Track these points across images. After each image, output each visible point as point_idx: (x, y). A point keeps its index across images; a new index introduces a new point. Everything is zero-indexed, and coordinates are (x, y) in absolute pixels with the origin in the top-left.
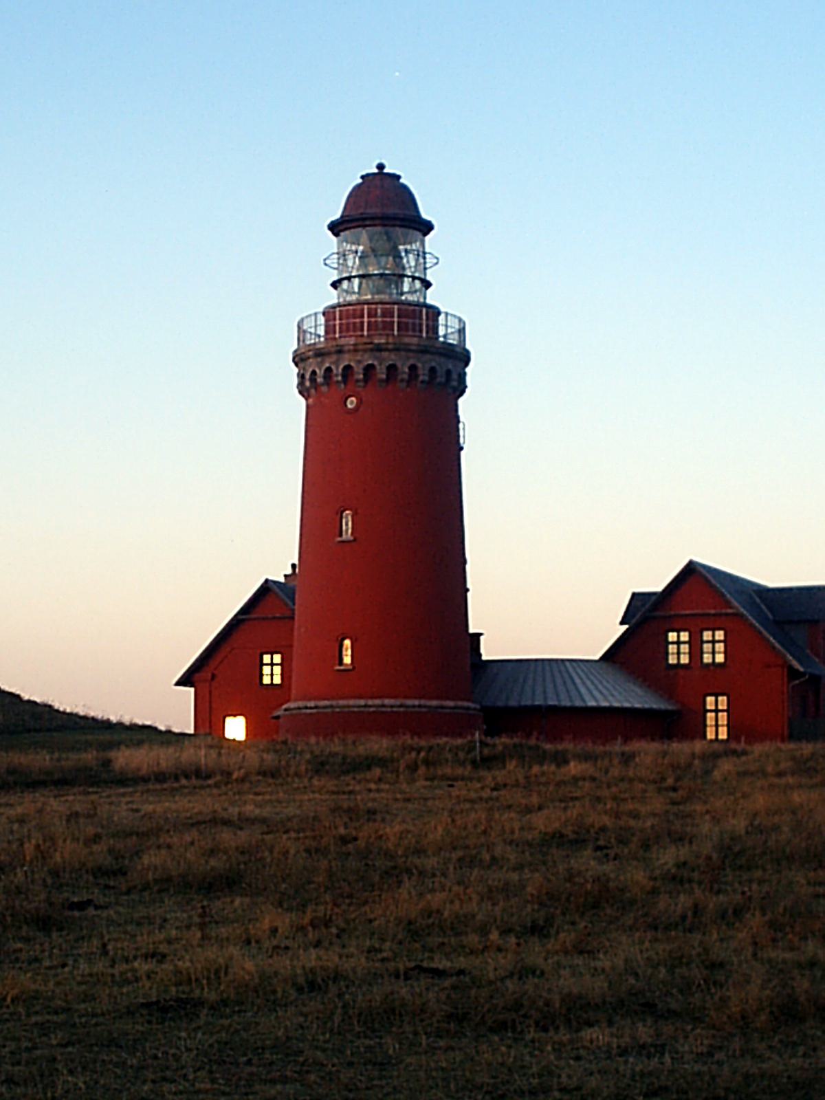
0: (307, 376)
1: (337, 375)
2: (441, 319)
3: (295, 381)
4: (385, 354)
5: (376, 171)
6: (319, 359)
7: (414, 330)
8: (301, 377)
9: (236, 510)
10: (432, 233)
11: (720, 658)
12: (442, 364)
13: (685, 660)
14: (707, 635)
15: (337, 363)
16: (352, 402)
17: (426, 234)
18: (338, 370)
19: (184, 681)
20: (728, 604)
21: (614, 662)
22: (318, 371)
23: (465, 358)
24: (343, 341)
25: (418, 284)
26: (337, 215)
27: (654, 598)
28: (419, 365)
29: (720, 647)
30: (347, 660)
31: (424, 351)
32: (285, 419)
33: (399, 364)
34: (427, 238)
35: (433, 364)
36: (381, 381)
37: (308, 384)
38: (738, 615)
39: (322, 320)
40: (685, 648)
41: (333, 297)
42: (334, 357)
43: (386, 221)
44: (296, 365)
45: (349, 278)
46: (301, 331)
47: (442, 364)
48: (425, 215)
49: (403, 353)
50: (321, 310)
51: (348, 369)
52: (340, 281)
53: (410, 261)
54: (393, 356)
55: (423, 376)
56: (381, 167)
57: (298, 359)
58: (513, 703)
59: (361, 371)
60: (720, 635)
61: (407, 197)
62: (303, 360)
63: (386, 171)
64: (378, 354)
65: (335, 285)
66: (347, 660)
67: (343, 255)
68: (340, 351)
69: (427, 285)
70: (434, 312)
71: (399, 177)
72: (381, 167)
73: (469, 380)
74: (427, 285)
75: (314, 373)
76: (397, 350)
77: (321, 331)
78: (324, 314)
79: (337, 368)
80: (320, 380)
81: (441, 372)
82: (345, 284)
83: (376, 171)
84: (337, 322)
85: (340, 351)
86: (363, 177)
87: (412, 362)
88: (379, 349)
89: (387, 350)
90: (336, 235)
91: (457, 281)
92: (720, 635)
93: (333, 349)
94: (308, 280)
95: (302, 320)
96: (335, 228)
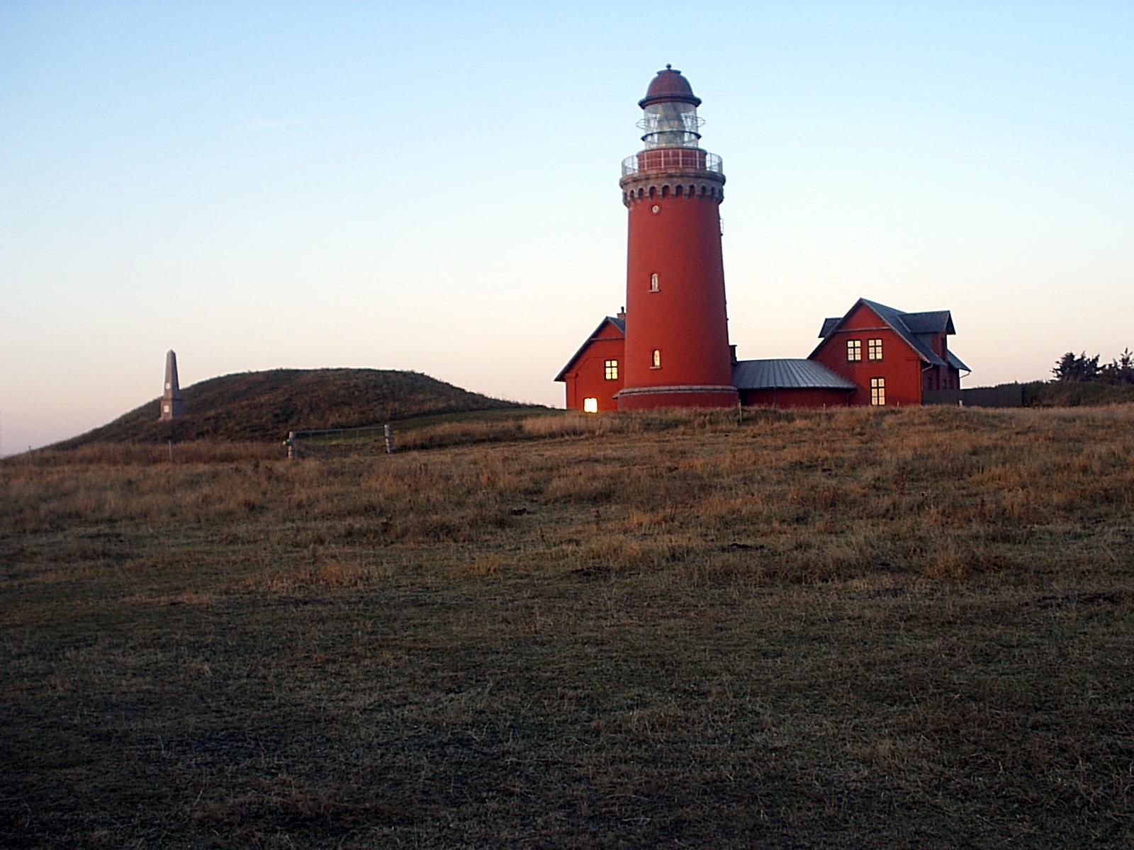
0: (629, 194)
2: (708, 157)
3: (621, 197)
4: (675, 179)
5: (666, 69)
7: (692, 164)
8: (625, 194)
9: (588, 277)
10: (701, 105)
11: (879, 356)
12: (710, 185)
13: (858, 358)
14: (871, 343)
15: (645, 185)
17: (697, 106)
18: (647, 190)
19: (560, 378)
20: (884, 324)
21: (816, 360)
23: (723, 181)
24: (649, 172)
25: (693, 137)
26: (643, 96)
27: (839, 322)
28: (695, 185)
29: (879, 349)
30: (657, 363)
31: (697, 177)
32: (617, 219)
33: (683, 185)
34: (698, 108)
35: (703, 184)
36: (672, 195)
37: (629, 198)
38: (890, 330)
39: (636, 160)
40: (858, 351)
41: (642, 146)
42: (644, 182)
43: (673, 99)
44: (622, 187)
45: (652, 134)
46: (624, 168)
47: (710, 185)
48: (696, 94)
50: (635, 154)
52: (646, 136)
53: (688, 124)
55: (698, 191)
56: (669, 66)
57: (623, 184)
58: (756, 386)
60: (879, 342)
61: (685, 84)
62: (625, 184)
63: (672, 68)
65: (643, 139)
66: (657, 363)
67: (648, 121)
69: (699, 137)
70: (703, 154)
71: (679, 72)
72: (669, 66)
73: (725, 194)
74: (699, 137)
75: (632, 192)
76: (682, 176)
77: (636, 167)
78: (637, 156)
80: (636, 196)
81: (709, 188)
82: (649, 138)
83: (666, 69)
85: (648, 179)
86: (658, 73)
87: (691, 183)
88: (671, 176)
89: (677, 177)
90: (643, 108)
91: (717, 134)
92: (879, 342)
94: (627, 136)
95: (624, 161)
96: (643, 104)
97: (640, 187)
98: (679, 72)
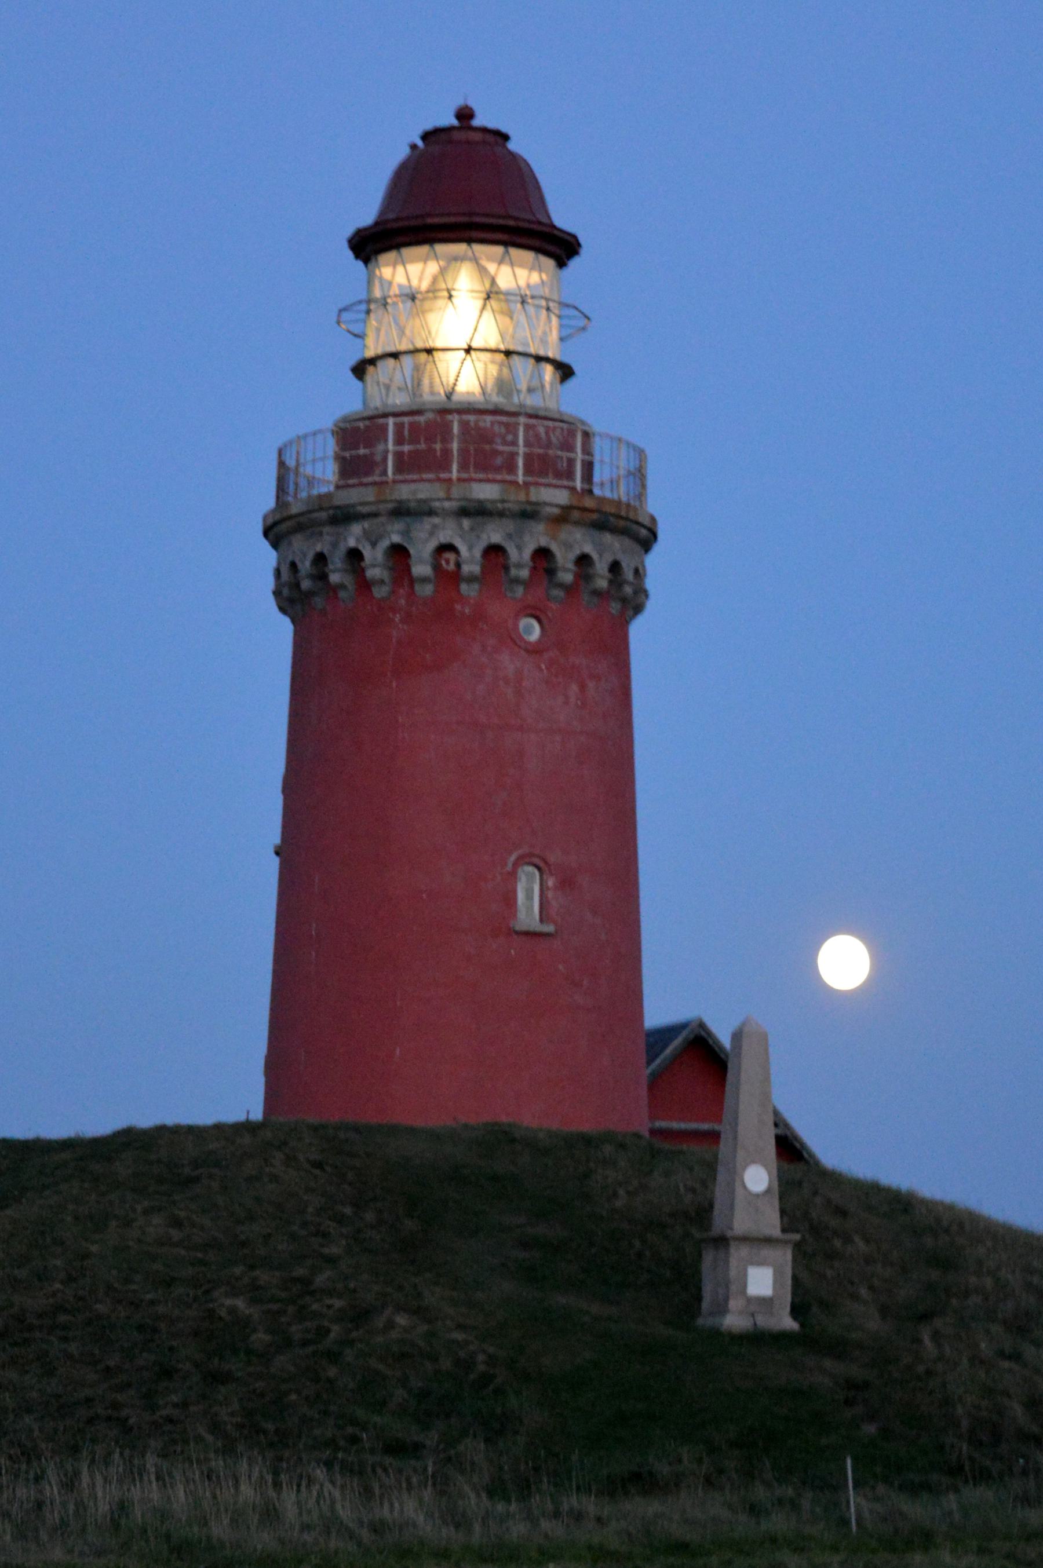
1: (519, 566)
4: (608, 538)
5: (455, 122)
6: (466, 523)
16: (529, 630)
18: (520, 556)
22: (463, 549)
42: (510, 525)
49: (627, 542)
51: (543, 554)
54: (617, 545)
56: (465, 115)
59: (571, 566)
63: (476, 122)
64: (596, 533)
68: (529, 514)
72: (465, 115)
83: (455, 122)
85: (529, 514)
93: (515, 508)
97: (496, 538)
98: (505, 137)
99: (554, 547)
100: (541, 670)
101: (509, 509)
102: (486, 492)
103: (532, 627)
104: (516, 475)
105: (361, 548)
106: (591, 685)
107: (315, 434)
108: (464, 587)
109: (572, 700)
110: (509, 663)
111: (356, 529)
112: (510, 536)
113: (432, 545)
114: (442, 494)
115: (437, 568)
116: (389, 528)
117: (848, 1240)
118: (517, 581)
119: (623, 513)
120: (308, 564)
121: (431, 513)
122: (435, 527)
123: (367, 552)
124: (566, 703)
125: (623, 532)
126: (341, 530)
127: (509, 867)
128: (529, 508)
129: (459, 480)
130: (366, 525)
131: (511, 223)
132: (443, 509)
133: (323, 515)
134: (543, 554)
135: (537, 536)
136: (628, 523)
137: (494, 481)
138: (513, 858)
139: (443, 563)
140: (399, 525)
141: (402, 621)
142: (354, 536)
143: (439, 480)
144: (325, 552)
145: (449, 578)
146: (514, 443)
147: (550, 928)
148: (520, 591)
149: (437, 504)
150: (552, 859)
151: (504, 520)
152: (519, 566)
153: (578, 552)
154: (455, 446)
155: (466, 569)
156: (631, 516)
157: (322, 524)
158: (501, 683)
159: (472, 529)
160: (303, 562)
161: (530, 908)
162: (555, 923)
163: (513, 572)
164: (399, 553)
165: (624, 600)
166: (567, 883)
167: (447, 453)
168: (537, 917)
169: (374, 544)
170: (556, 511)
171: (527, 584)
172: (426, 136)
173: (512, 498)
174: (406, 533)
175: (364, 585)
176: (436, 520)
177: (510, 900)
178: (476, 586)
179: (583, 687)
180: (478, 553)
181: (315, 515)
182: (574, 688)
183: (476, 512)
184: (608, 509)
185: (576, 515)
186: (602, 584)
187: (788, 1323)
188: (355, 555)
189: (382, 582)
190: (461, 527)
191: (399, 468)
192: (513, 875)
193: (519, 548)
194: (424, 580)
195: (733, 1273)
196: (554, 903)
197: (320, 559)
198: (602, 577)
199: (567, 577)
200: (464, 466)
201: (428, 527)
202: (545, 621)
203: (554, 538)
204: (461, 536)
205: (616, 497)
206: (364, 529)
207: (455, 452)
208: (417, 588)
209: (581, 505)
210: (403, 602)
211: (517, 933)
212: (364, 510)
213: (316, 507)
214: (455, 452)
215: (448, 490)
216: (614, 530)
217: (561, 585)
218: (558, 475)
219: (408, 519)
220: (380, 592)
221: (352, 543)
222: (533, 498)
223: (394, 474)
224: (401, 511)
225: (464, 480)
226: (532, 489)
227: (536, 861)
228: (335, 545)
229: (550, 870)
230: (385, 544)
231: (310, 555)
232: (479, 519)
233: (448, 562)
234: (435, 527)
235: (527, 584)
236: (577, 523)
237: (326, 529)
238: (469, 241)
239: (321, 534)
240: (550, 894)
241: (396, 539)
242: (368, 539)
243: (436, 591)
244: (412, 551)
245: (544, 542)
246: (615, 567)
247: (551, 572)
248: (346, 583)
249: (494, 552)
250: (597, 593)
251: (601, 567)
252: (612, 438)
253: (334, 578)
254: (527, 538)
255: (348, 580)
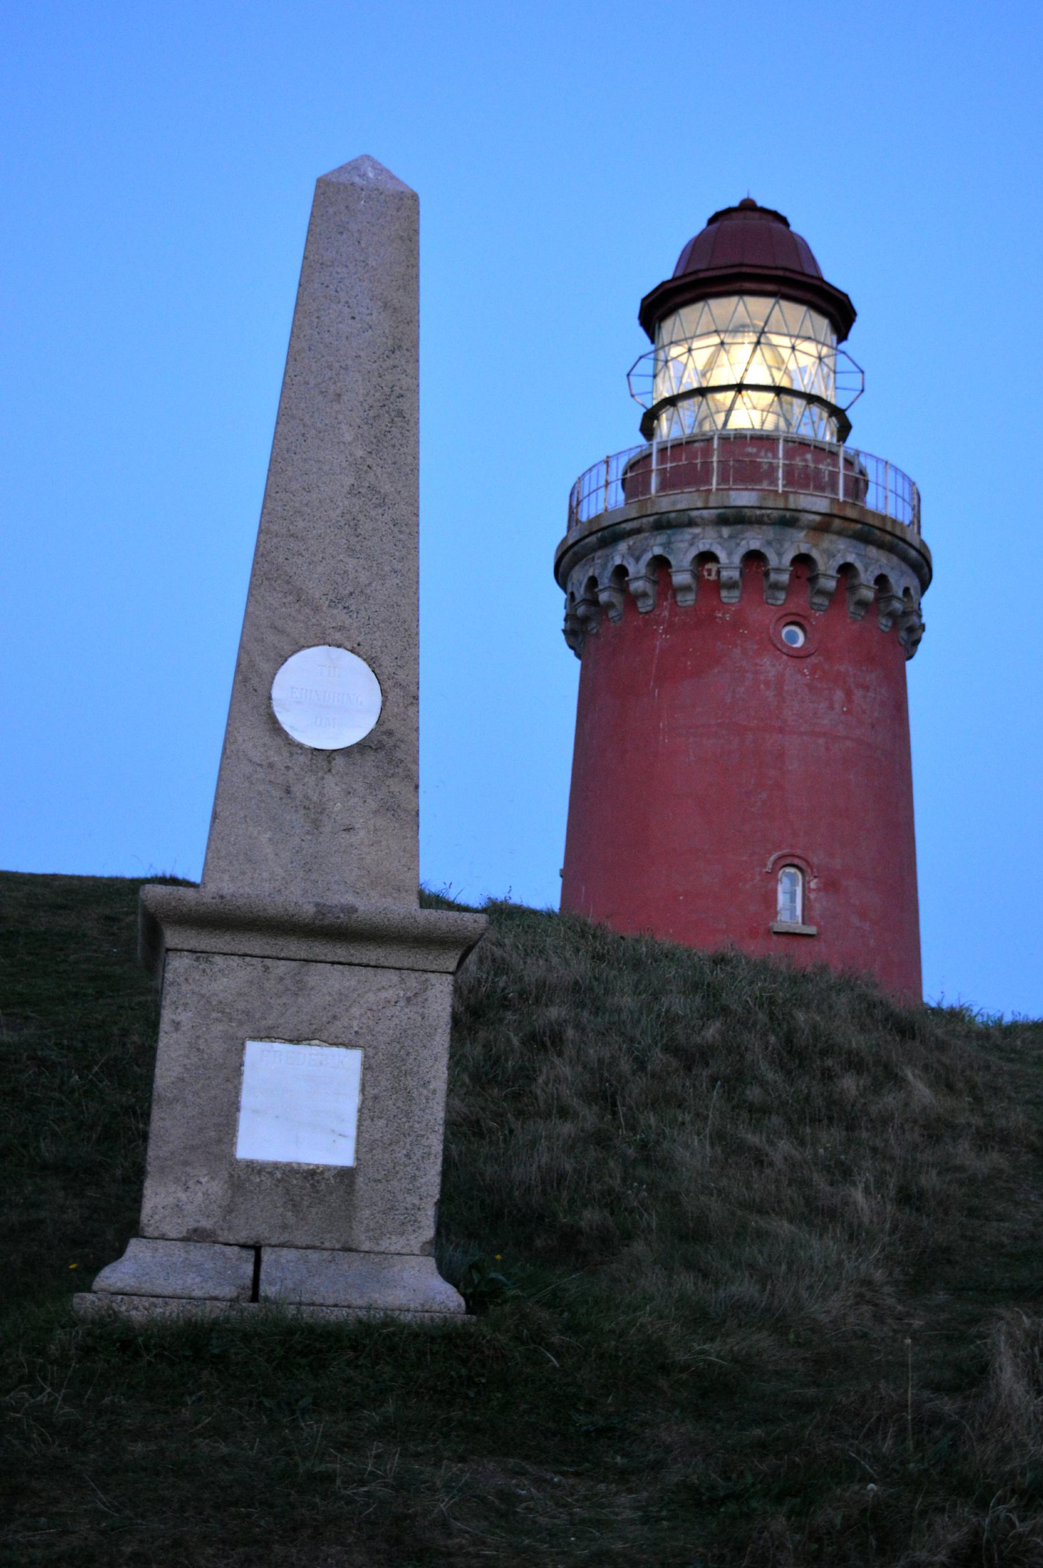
1: (778, 570)
4: (873, 551)
6: (726, 531)
16: (793, 637)
26: (663, 268)
33: (893, 578)
42: (770, 532)
49: (895, 560)
51: (803, 561)
64: (862, 546)
68: (788, 521)
79: (780, 555)
84: (781, 462)
85: (788, 521)
93: (775, 514)
97: (755, 545)
99: (815, 554)
100: (806, 676)
101: (768, 516)
102: (744, 498)
103: (795, 633)
104: (777, 485)
105: (625, 564)
106: (858, 694)
107: (590, 470)
108: (724, 593)
109: (837, 706)
110: (770, 666)
111: (623, 547)
112: (769, 543)
113: (693, 553)
114: (700, 505)
115: (697, 576)
116: (652, 542)
117: (889, 1077)
118: (776, 586)
119: (889, 528)
120: (582, 590)
121: (691, 523)
122: (695, 536)
123: (632, 569)
124: (831, 707)
125: (891, 549)
126: (607, 551)
127: (769, 867)
128: (788, 514)
129: (717, 490)
130: (631, 541)
131: (780, 273)
132: (703, 519)
133: (593, 539)
134: (803, 561)
135: (798, 543)
136: (896, 541)
137: (753, 489)
138: (772, 858)
139: (705, 573)
140: (661, 538)
141: (666, 632)
142: (619, 555)
143: (698, 491)
144: (596, 575)
145: (709, 588)
146: (775, 456)
147: (812, 930)
148: (782, 596)
149: (695, 513)
150: (815, 860)
151: (764, 527)
152: (778, 570)
153: (842, 562)
154: (715, 459)
155: (725, 574)
156: (898, 533)
157: (594, 549)
158: (762, 686)
159: (731, 537)
160: (578, 590)
161: (793, 910)
162: (818, 925)
163: (773, 577)
164: (661, 564)
165: (891, 615)
166: (831, 885)
167: (707, 465)
168: (800, 920)
169: (637, 559)
170: (818, 518)
171: (788, 589)
172: (712, 221)
173: (770, 504)
174: (667, 545)
175: (631, 600)
176: (697, 530)
177: (769, 900)
178: (736, 593)
179: (849, 694)
180: (737, 560)
181: (587, 540)
182: (839, 695)
183: (734, 519)
184: (870, 520)
185: (837, 523)
186: (869, 595)
187: (418, 1287)
188: (621, 571)
189: (645, 595)
190: (721, 536)
191: (663, 486)
192: (772, 876)
193: (780, 555)
194: (686, 589)
195: (171, 1060)
196: (817, 906)
197: (593, 582)
198: (868, 587)
199: (831, 584)
200: (723, 479)
201: (688, 537)
202: (808, 628)
203: (816, 546)
204: (720, 544)
205: (883, 512)
206: (630, 548)
207: (715, 465)
208: (679, 598)
209: (841, 514)
210: (666, 613)
211: (776, 933)
212: (628, 526)
213: (586, 533)
214: (715, 465)
215: (707, 501)
216: (880, 545)
217: (821, 592)
218: (820, 487)
219: (669, 532)
220: (644, 606)
221: (618, 561)
222: (792, 506)
223: (657, 491)
224: (663, 524)
225: (723, 490)
226: (791, 497)
227: (796, 861)
228: (604, 566)
229: (812, 872)
230: (647, 557)
231: (585, 581)
232: (739, 527)
233: (709, 571)
234: (695, 536)
235: (788, 589)
236: (840, 533)
237: (599, 553)
238: (741, 293)
239: (593, 559)
240: (812, 896)
241: (658, 551)
242: (632, 555)
243: (696, 600)
244: (673, 562)
245: (804, 549)
246: (881, 580)
247: (813, 579)
248: (614, 600)
249: (754, 558)
250: (862, 603)
251: (866, 577)
252: (878, 460)
253: (603, 597)
254: (787, 545)
255: (617, 599)
